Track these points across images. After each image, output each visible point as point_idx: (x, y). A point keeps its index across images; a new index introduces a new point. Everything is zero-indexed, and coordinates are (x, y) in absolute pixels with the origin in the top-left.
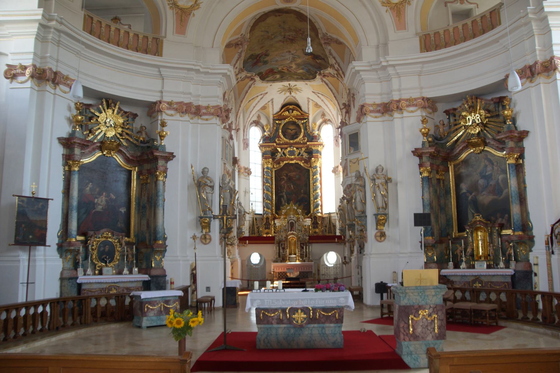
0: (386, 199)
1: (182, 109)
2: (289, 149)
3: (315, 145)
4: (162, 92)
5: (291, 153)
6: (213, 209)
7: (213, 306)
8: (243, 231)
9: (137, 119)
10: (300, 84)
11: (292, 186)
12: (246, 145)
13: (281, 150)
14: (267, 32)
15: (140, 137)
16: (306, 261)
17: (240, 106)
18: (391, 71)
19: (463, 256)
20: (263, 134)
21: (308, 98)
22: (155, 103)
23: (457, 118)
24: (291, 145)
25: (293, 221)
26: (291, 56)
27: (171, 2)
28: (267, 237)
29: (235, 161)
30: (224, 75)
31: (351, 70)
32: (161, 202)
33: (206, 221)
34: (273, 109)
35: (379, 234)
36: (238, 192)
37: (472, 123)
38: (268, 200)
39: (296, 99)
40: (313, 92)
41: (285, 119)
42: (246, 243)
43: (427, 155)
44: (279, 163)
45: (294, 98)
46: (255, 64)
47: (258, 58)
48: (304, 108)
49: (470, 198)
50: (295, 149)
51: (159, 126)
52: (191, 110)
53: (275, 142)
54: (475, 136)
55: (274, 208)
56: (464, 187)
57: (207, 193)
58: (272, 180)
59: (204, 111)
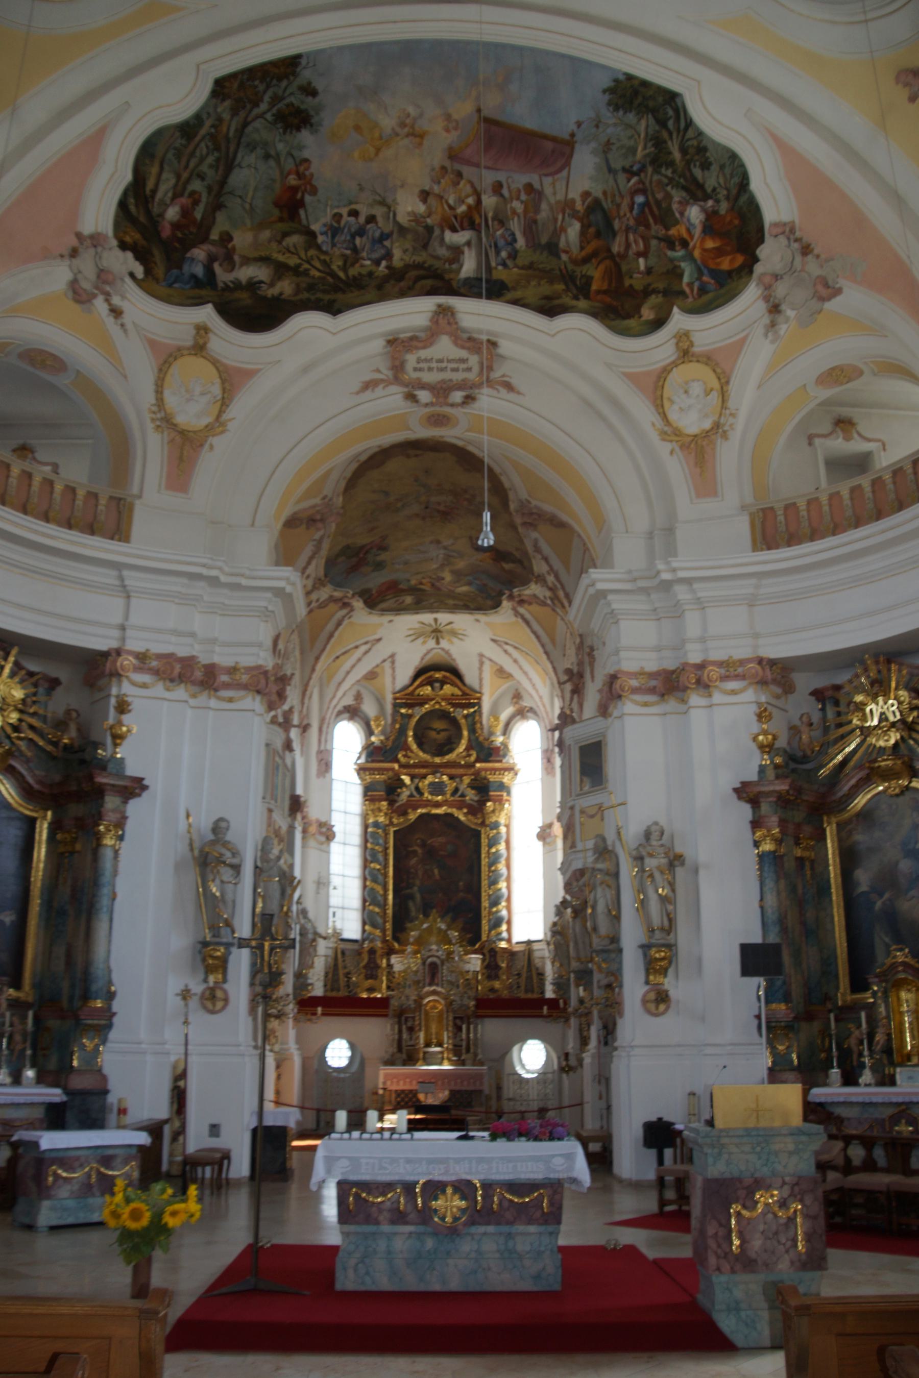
0: (670, 908)
1: (173, 669)
2: (430, 779)
3: (495, 770)
4: (123, 628)
5: (437, 788)
6: (236, 923)
7: (224, 1176)
8: (310, 981)
9: (59, 691)
10: (462, 621)
11: (436, 871)
12: (325, 765)
13: (412, 780)
14: (387, 494)
15: (62, 736)
17: (313, 670)
18: (682, 593)
19: (866, 1053)
21: (481, 656)
22: (105, 655)
23: (842, 708)
24: (435, 769)
25: (435, 959)
26: (442, 551)
27: (159, 416)
28: (368, 998)
29: (296, 805)
30: (279, 592)
31: (586, 590)
32: (105, 901)
33: (219, 954)
34: (394, 678)
35: (652, 996)
36: (299, 882)
37: (880, 721)
40: (493, 640)
41: (422, 704)
42: (315, 1014)
43: (771, 799)
45: (447, 652)
46: (354, 569)
47: (361, 555)
48: (470, 678)
49: (879, 905)
50: (445, 778)
51: (112, 711)
52: (192, 674)
53: (397, 760)
54: (889, 752)
55: (389, 926)
56: (863, 878)
57: (222, 882)
59: (224, 678)
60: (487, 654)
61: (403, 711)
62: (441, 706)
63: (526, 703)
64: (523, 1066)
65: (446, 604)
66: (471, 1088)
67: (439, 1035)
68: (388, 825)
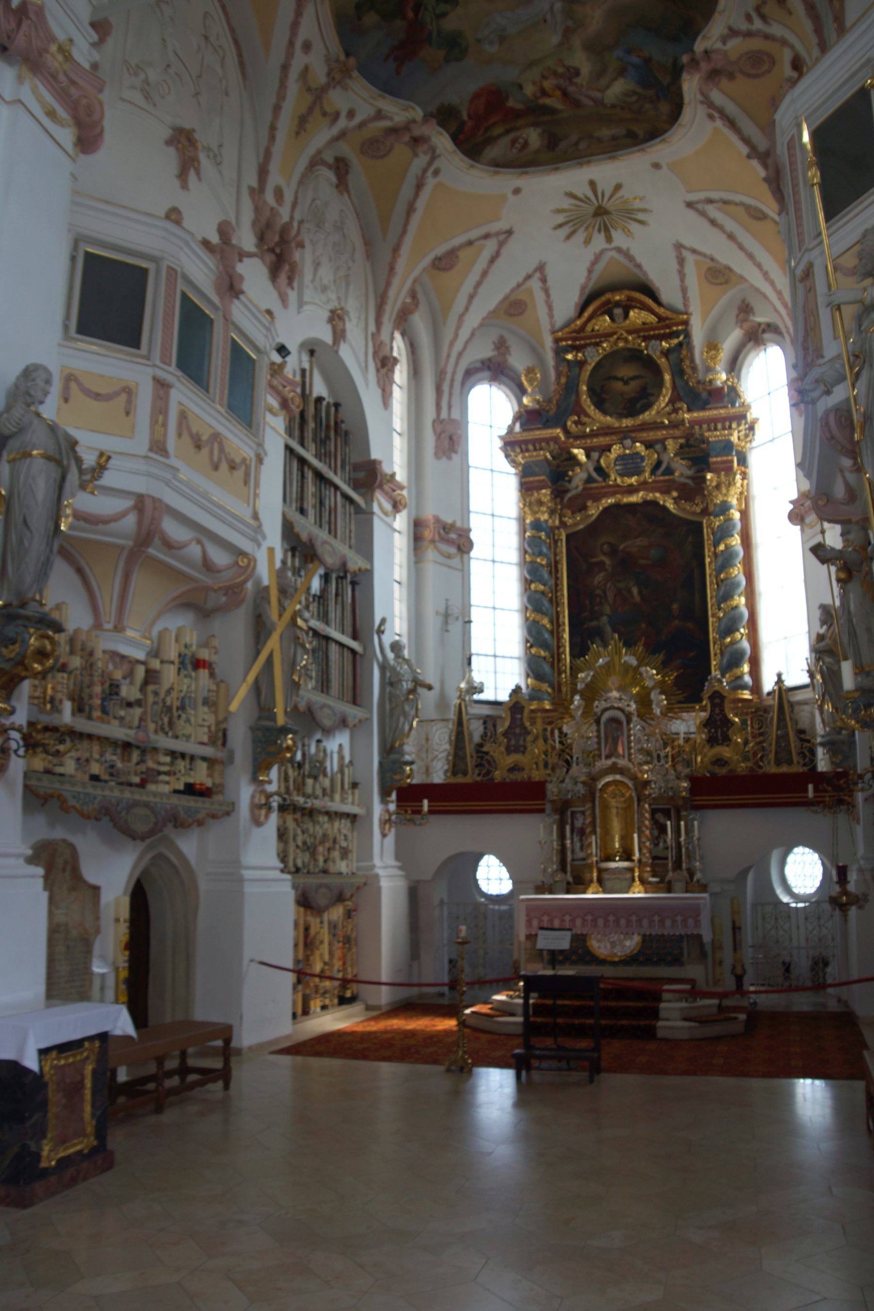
2: (616, 450)
5: (630, 465)
8: (407, 758)
11: (635, 591)
13: (588, 456)
16: (678, 885)
17: (392, 269)
20: (520, 402)
21: (679, 247)
24: (624, 435)
34: (550, 307)
39: (631, 259)
40: (690, 205)
41: (598, 344)
42: (419, 812)
44: (584, 508)
45: (627, 254)
48: (669, 293)
58: (557, 571)
60: (687, 243)
61: (569, 357)
62: (626, 340)
64: (788, 889)
65: (599, 140)
66: (679, 931)
67: (626, 839)
68: (558, 528)
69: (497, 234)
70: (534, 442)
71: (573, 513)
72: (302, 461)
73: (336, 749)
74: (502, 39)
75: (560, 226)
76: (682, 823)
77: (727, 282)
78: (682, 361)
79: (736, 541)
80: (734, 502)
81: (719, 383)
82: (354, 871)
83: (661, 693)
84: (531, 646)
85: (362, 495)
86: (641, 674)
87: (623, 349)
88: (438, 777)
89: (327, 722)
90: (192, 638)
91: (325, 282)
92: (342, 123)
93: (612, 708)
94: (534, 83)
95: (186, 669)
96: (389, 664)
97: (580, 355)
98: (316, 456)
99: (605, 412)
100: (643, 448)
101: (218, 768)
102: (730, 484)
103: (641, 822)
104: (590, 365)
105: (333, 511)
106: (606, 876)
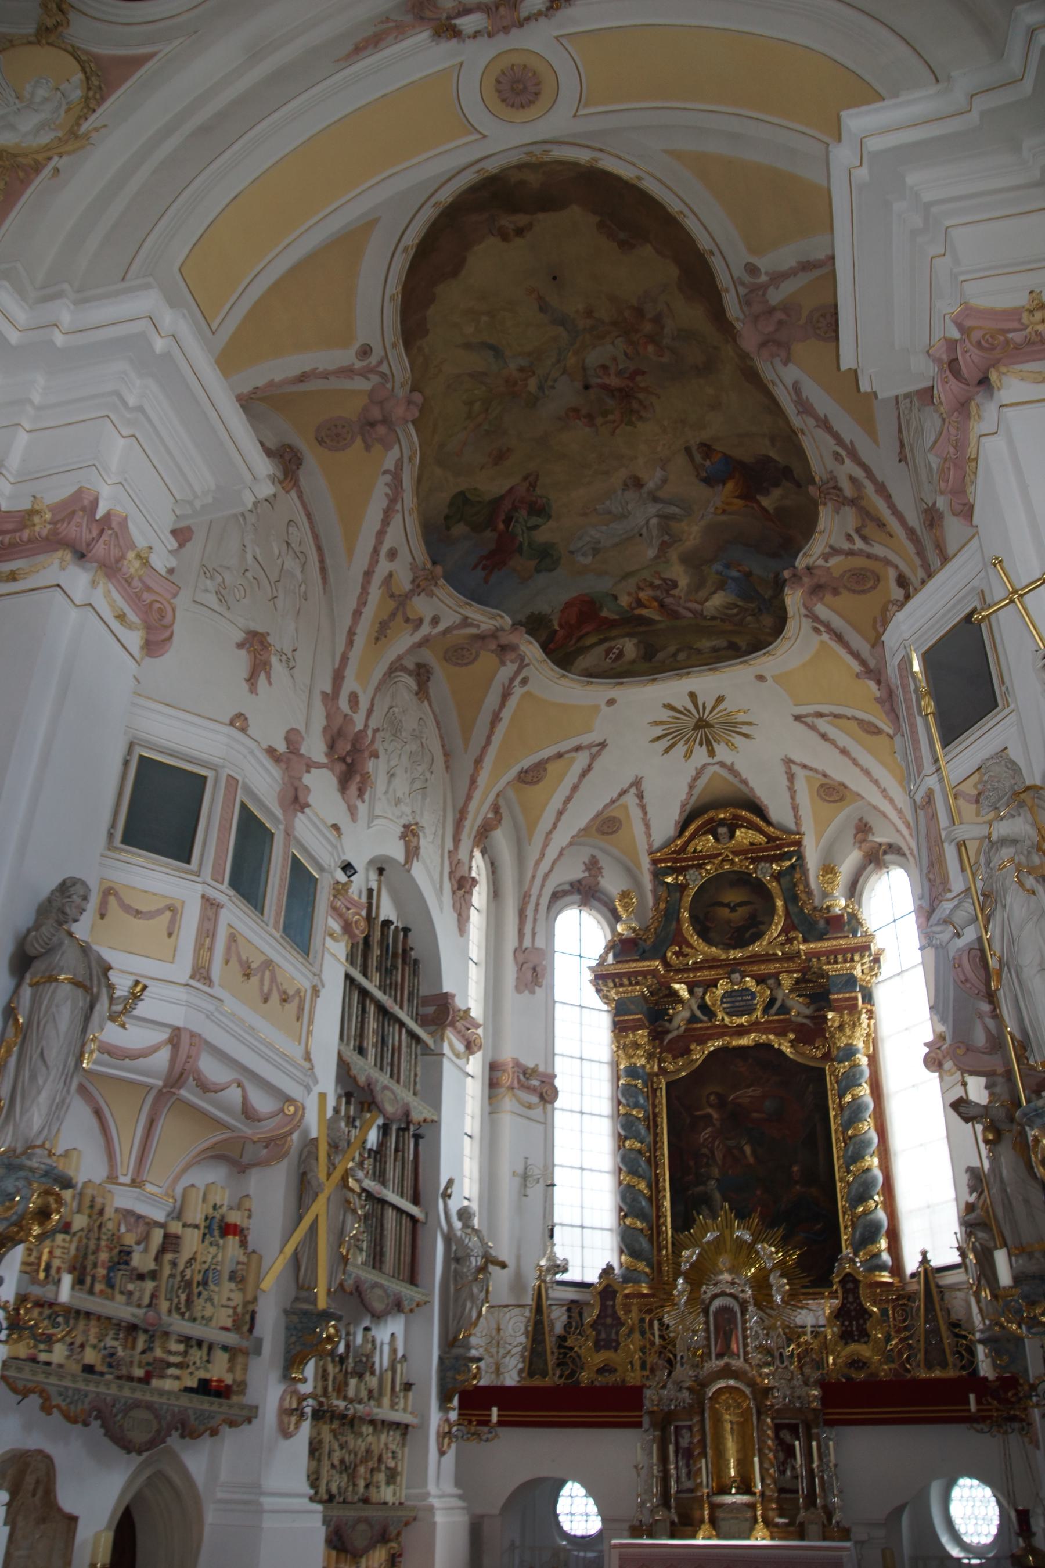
5: (739, 1002)
8: (474, 1353)
11: (748, 1150)
13: (691, 992)
14: (496, 351)
17: (473, 781)
20: (613, 930)
21: (788, 762)
24: (732, 968)
26: (653, 509)
34: (647, 826)
38: (637, 1216)
39: (736, 774)
40: (798, 718)
41: (700, 866)
42: (486, 1423)
44: (688, 1051)
45: (731, 769)
48: (779, 811)
58: (656, 1126)
61: (669, 880)
62: (732, 862)
63: (881, 837)
65: (699, 651)
68: (657, 1075)
69: (590, 746)
70: (629, 975)
71: (675, 1057)
72: (364, 993)
73: (387, 1339)
74: (596, 551)
75: (659, 738)
76: (814, 1443)
77: (842, 799)
78: (795, 885)
79: (864, 1090)
80: (861, 1045)
81: (837, 910)
82: (403, 1500)
83: (782, 1276)
84: (625, 1216)
85: (431, 1033)
86: (757, 1252)
87: (729, 872)
88: (511, 1379)
89: (378, 1306)
90: (222, 1197)
91: (399, 794)
92: (425, 629)
93: (723, 1294)
94: (629, 594)
95: (212, 1236)
96: (455, 1235)
97: (681, 878)
98: (380, 988)
99: (709, 942)
100: (754, 983)
101: (240, 1359)
102: (854, 1025)
103: (762, 1442)
104: (692, 889)
105: (396, 1051)
106: (720, 1514)
